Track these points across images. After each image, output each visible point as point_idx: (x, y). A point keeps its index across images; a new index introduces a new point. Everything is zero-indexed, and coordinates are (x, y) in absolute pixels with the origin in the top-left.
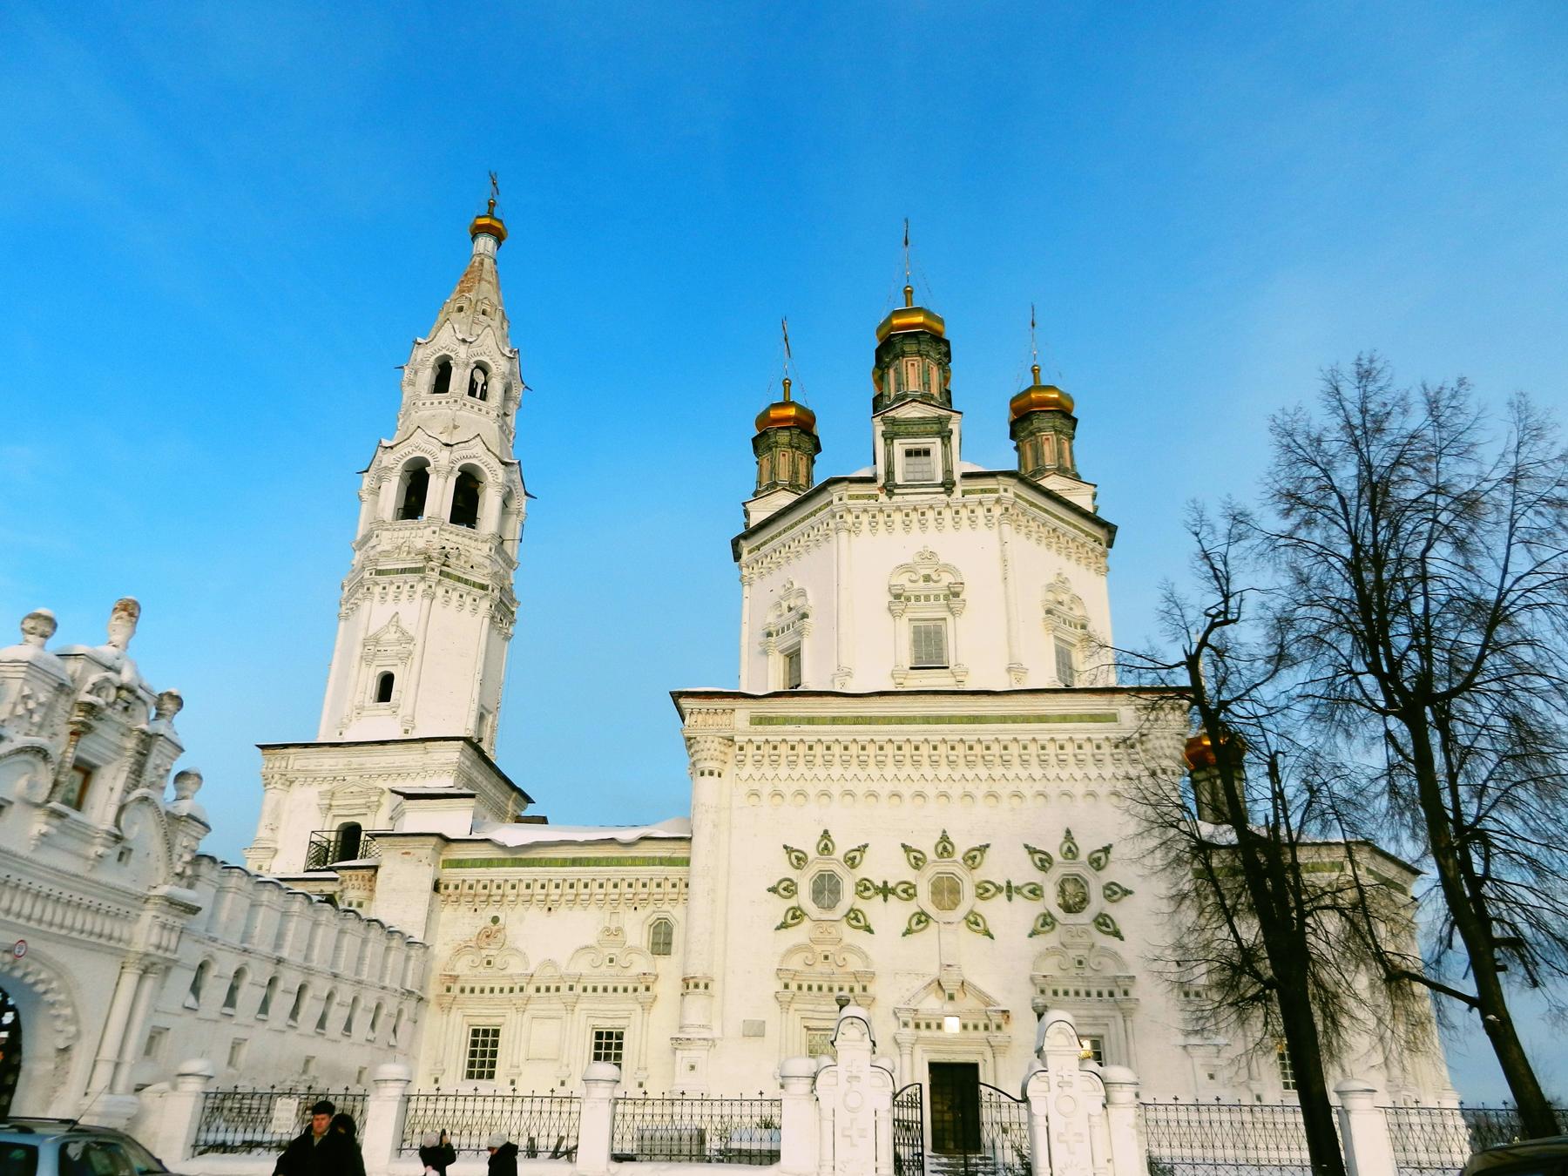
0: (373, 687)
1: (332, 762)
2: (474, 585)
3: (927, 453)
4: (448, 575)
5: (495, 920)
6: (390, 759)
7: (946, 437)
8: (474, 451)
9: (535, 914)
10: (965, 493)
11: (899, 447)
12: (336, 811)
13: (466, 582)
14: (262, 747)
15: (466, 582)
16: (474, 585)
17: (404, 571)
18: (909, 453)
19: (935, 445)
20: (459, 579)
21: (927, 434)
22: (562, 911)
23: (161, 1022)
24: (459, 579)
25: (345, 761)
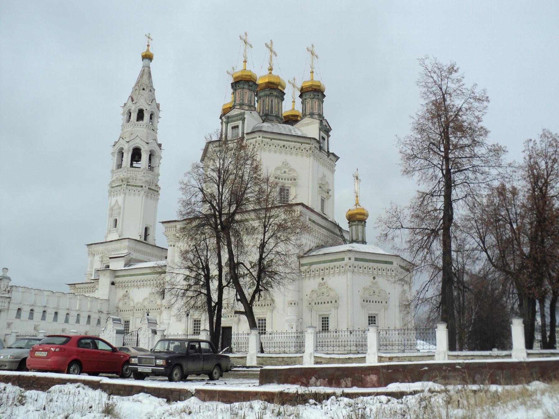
0: (113, 223)
1: (101, 248)
2: (138, 186)
3: (237, 127)
4: (129, 185)
5: (127, 291)
6: (113, 246)
7: (243, 120)
8: (137, 142)
9: (135, 290)
10: (247, 140)
11: (230, 126)
12: (104, 262)
13: (136, 186)
14: (88, 245)
15: (136, 186)
16: (138, 186)
17: (117, 186)
18: (233, 128)
19: (240, 123)
20: (133, 186)
21: (237, 120)
22: (141, 289)
23: (11, 321)
24: (133, 186)
25: (104, 247)
